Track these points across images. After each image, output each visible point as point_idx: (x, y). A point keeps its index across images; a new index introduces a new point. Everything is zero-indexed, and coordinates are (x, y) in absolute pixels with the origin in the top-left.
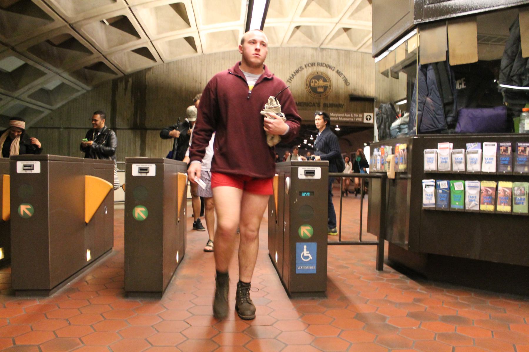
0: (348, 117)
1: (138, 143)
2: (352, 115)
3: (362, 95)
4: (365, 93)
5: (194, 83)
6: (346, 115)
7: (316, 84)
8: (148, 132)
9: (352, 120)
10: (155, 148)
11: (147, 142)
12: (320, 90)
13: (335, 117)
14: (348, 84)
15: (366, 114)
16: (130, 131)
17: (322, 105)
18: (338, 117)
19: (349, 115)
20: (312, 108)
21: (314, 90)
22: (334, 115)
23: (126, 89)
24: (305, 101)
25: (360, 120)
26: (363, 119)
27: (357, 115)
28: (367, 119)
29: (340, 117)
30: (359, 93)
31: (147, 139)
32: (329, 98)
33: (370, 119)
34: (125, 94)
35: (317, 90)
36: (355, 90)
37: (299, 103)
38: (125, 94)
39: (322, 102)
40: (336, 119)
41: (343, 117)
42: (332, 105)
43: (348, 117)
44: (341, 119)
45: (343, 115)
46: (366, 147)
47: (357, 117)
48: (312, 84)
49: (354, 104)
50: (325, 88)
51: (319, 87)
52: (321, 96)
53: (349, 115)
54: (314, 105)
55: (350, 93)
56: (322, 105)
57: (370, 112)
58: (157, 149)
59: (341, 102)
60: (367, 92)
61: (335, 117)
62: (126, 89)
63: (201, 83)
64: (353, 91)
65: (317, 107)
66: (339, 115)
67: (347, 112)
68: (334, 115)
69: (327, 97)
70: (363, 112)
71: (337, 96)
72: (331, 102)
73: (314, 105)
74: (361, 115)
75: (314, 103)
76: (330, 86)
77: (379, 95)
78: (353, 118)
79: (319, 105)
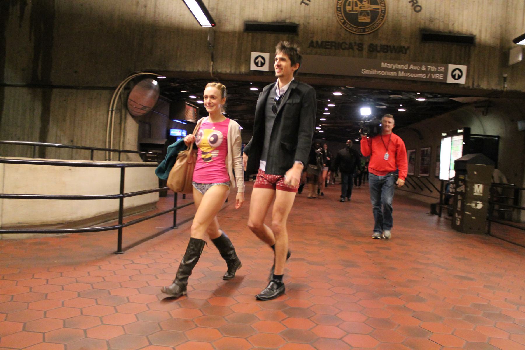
0: (416, 72)
1: (38, 111)
2: (424, 68)
3: (446, 31)
4: (451, 28)
5: (134, 7)
6: (412, 67)
7: (356, 9)
8: (55, 91)
9: (424, 76)
10: (64, 120)
11: (52, 109)
12: (362, 19)
13: (391, 70)
14: (418, 8)
15: (451, 67)
16: (25, 90)
17: (366, 47)
18: (397, 70)
19: (418, 68)
20: (346, 52)
21: (352, 18)
22: (389, 66)
23: (21, 17)
24: (333, 39)
25: (440, 77)
26: (445, 77)
27: (433, 68)
28: (454, 77)
29: (402, 70)
30: (439, 26)
31: (52, 104)
32: (380, 35)
33: (460, 77)
34: (20, 27)
35: (357, 18)
36: (431, 20)
37: (322, 42)
38: (20, 27)
39: (367, 40)
40: (392, 74)
41: (406, 71)
42: (386, 49)
43: (416, 72)
44: (401, 74)
45: (406, 67)
46: (446, 139)
47: (434, 72)
48: (349, 8)
49: (429, 46)
50: (374, 15)
51: (361, 13)
52: (364, 31)
53: (418, 68)
54: (351, 47)
55: (422, 26)
56: (366, 47)
57: (460, 64)
58: (68, 121)
59: (403, 44)
60: (456, 25)
61: (391, 70)
62: (21, 17)
63: (145, 6)
64: (427, 23)
65: (357, 52)
66: (399, 67)
67: (415, 60)
68: (389, 66)
69: (376, 33)
70: (447, 62)
71: (396, 31)
72: (384, 43)
73: (351, 47)
74: (441, 69)
75: (351, 44)
76: (384, 12)
77: (480, 31)
78: (426, 72)
79: (360, 47)
